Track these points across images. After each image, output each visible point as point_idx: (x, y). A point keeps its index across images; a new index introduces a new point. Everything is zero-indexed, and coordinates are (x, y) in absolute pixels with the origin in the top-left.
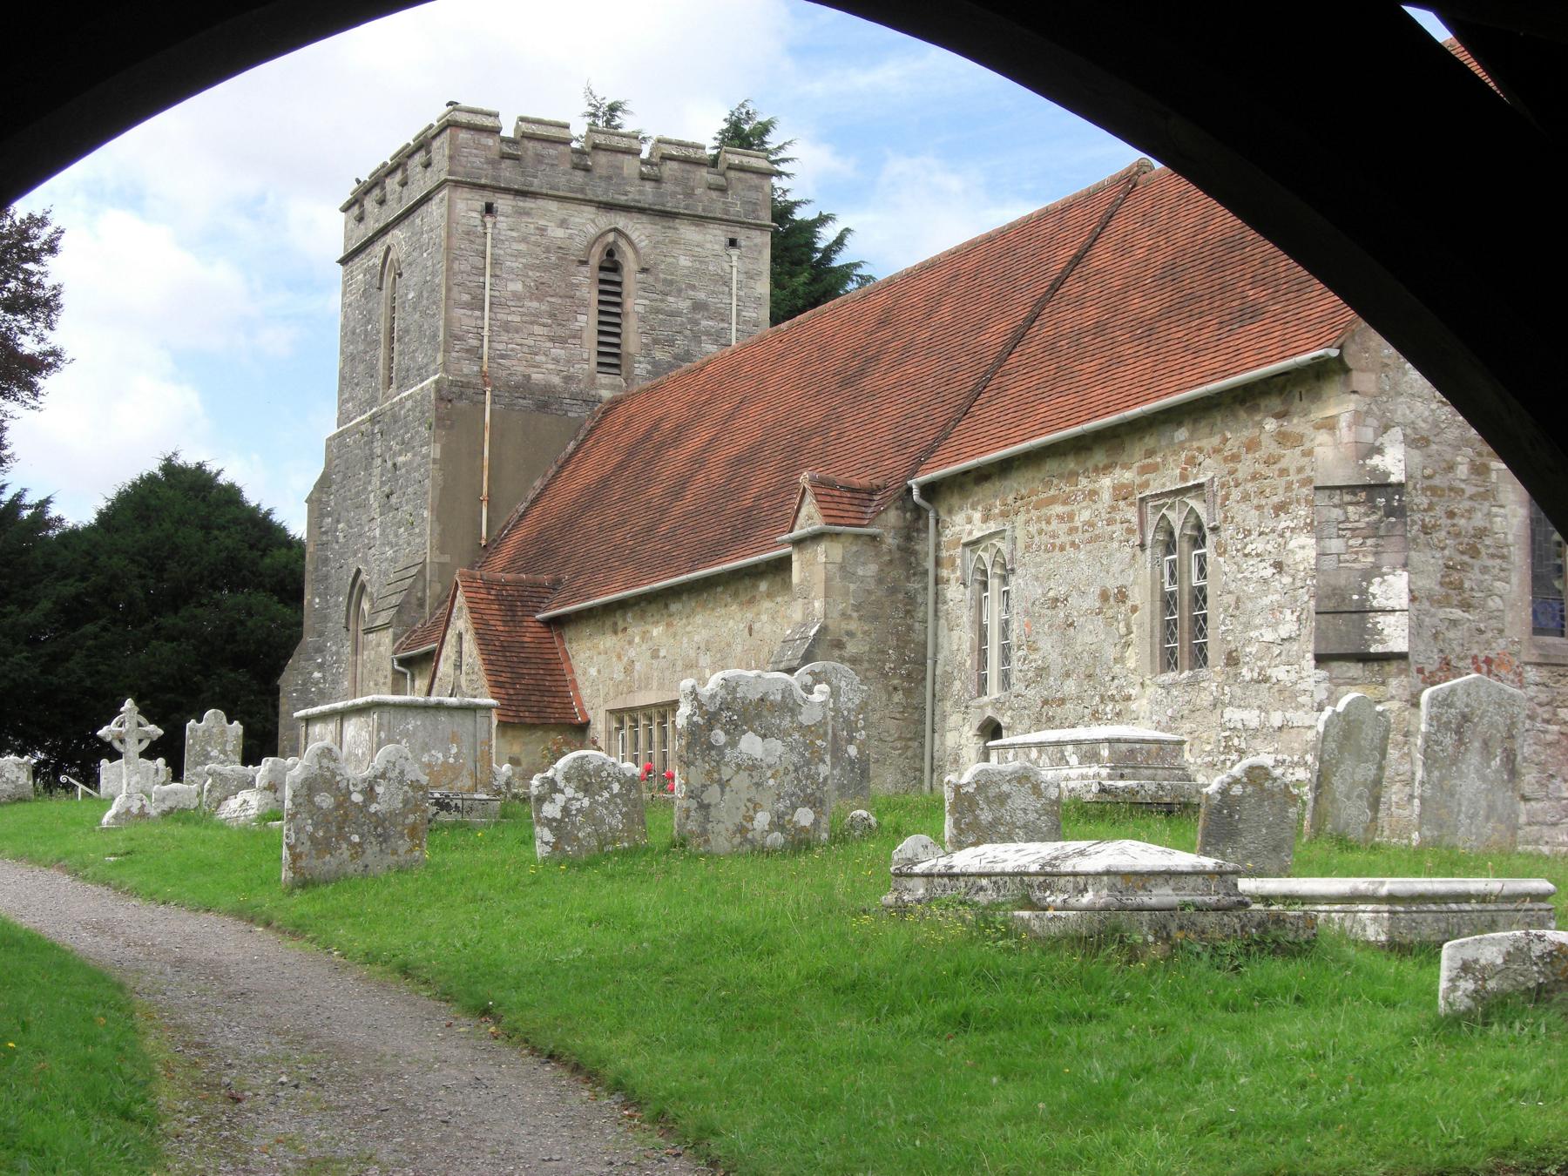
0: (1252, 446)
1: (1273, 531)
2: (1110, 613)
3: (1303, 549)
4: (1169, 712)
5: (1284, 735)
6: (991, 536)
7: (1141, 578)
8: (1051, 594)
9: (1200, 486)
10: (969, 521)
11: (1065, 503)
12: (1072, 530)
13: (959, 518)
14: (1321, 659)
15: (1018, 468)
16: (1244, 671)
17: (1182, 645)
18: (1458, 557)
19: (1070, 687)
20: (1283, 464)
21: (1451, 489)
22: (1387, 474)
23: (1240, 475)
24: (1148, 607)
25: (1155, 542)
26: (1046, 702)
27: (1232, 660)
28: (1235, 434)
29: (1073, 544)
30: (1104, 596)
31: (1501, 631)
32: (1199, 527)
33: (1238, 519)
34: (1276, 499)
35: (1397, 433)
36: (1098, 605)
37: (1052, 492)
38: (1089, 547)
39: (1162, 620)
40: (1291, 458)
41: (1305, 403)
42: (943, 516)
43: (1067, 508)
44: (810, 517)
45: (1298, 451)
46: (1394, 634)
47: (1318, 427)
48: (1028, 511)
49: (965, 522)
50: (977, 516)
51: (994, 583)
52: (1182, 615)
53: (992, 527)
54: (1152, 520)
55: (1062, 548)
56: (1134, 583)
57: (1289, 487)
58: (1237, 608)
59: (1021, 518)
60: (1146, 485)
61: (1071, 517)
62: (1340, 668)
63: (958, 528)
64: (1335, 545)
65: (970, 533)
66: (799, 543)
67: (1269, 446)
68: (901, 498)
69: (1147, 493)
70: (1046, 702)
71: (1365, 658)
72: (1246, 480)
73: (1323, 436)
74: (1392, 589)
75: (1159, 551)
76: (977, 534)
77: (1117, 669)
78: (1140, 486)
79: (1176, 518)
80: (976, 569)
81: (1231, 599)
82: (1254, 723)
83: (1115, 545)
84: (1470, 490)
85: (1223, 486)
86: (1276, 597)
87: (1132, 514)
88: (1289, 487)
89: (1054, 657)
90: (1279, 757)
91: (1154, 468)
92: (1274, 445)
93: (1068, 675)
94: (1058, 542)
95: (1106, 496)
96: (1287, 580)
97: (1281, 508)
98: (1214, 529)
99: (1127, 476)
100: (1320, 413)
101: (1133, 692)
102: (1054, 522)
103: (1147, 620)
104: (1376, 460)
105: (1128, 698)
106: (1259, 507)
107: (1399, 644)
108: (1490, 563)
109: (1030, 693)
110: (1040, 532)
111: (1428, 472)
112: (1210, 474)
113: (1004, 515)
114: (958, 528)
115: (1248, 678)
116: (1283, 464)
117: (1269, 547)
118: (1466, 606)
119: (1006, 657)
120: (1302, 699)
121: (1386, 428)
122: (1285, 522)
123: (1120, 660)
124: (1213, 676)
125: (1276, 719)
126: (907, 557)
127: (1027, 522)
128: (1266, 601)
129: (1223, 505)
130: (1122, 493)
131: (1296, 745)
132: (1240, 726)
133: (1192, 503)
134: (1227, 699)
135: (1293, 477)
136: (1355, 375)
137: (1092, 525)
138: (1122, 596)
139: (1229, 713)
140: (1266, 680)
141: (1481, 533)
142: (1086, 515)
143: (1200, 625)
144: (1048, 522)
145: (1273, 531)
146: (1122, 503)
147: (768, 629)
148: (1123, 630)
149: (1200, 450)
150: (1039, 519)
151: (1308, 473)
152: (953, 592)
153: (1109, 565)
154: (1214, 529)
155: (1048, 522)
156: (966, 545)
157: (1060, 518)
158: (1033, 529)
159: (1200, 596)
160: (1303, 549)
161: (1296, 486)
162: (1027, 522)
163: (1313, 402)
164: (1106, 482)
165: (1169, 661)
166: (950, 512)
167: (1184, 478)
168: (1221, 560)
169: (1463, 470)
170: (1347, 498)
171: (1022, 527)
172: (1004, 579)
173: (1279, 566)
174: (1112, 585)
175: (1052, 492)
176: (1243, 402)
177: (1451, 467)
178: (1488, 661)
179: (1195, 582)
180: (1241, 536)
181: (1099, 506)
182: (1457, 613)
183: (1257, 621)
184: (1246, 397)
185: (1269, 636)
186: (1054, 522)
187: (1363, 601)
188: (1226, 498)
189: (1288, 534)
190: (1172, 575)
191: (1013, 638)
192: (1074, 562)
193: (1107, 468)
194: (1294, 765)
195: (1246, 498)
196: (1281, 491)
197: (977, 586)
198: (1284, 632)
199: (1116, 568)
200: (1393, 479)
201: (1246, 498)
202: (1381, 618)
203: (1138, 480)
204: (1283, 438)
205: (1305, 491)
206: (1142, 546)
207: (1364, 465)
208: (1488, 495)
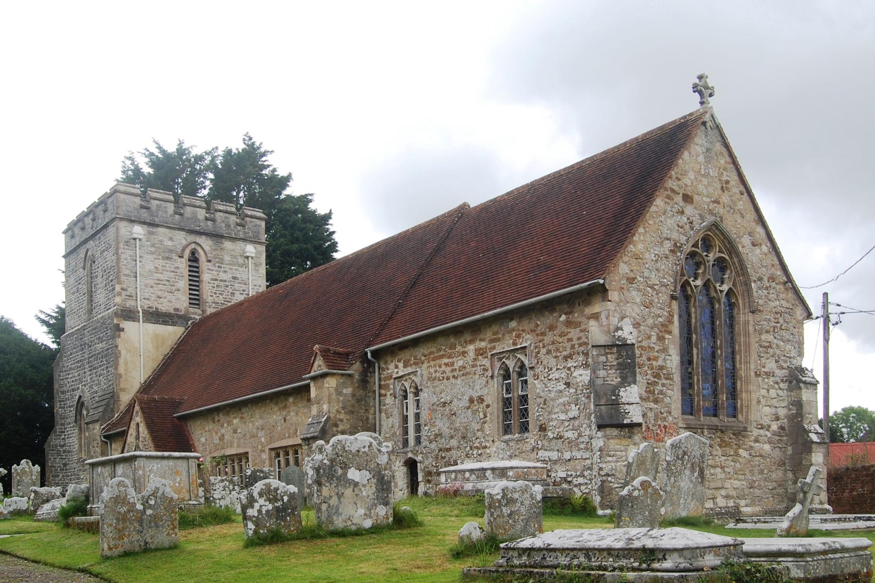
0: (552, 328)
1: (564, 368)
2: (475, 408)
3: (583, 376)
4: (508, 453)
5: (571, 462)
6: (409, 374)
7: (492, 392)
8: (442, 400)
9: (525, 348)
10: (397, 367)
11: (449, 357)
12: (452, 371)
13: (391, 366)
14: (600, 427)
15: (423, 342)
16: (549, 434)
17: (515, 422)
18: (652, 379)
19: (454, 443)
20: (569, 336)
21: (649, 347)
22: (625, 339)
23: (545, 342)
24: (495, 405)
25: (499, 374)
26: (440, 450)
27: (543, 429)
28: (543, 322)
29: (454, 377)
30: (471, 400)
31: (670, 413)
32: (522, 366)
33: (545, 362)
34: (565, 353)
35: (627, 320)
36: (468, 405)
37: (442, 353)
38: (463, 378)
39: (518, 409)
40: (574, 333)
41: (581, 307)
42: (382, 365)
43: (451, 360)
44: (319, 366)
45: (578, 330)
46: (635, 415)
47: (589, 318)
48: (429, 362)
49: (395, 368)
50: (401, 365)
51: (410, 396)
52: (514, 409)
53: (409, 370)
54: (498, 365)
55: (448, 379)
56: (488, 394)
57: (573, 347)
58: (545, 404)
59: (425, 365)
60: (494, 348)
61: (452, 364)
62: (609, 431)
63: (390, 371)
64: (602, 373)
65: (397, 373)
67: (561, 328)
68: (361, 357)
69: (495, 352)
70: (440, 450)
71: (621, 426)
72: (549, 344)
73: (592, 323)
74: (631, 394)
75: (501, 379)
76: (401, 374)
77: (479, 434)
78: (490, 349)
79: (511, 364)
80: (400, 389)
81: (543, 400)
82: (555, 458)
83: (477, 376)
84: (657, 348)
85: (536, 347)
86: (567, 399)
87: (486, 362)
88: (573, 347)
89: (446, 431)
90: (569, 473)
91: (498, 340)
92: (564, 327)
93: (452, 437)
94: (445, 375)
95: (472, 354)
96: (572, 390)
97: (566, 358)
98: (532, 368)
99: (483, 344)
100: (589, 311)
101: (488, 445)
102: (443, 367)
103: (495, 411)
104: (620, 333)
105: (486, 447)
106: (556, 357)
107: (637, 419)
108: (665, 382)
110: (436, 372)
111: (640, 339)
112: (529, 342)
113: (415, 364)
114: (390, 371)
115: (551, 437)
116: (569, 336)
117: (562, 376)
118: (656, 401)
119: (418, 428)
120: (582, 446)
121: (622, 318)
122: (570, 363)
123: (481, 430)
124: (532, 438)
125: (567, 455)
126: (364, 382)
127: (428, 367)
128: (561, 401)
129: (536, 356)
130: (480, 352)
131: (578, 468)
132: (547, 459)
133: (519, 356)
134: (540, 447)
135: (575, 342)
136: (610, 293)
137: (465, 367)
138: (481, 400)
139: (541, 453)
140: (561, 437)
141: (661, 368)
142: (460, 363)
143: (524, 413)
144: (440, 367)
145: (564, 368)
146: (480, 357)
148: (482, 416)
149: (523, 331)
150: (435, 366)
151: (584, 340)
152: (389, 400)
153: (474, 386)
154: (532, 368)
155: (440, 367)
156: (395, 379)
157: (446, 365)
158: (432, 370)
159: (524, 399)
160: (583, 376)
161: (577, 346)
162: (428, 367)
163: (586, 306)
165: (507, 430)
166: (386, 363)
167: (515, 344)
168: (536, 382)
169: (654, 339)
170: (608, 351)
171: (424, 370)
172: (416, 394)
173: (568, 384)
174: (475, 395)
175: (442, 353)
176: (546, 308)
177: (649, 337)
178: (665, 427)
179: (520, 393)
180: (547, 370)
181: (468, 358)
182: (652, 405)
183: (556, 410)
184: (549, 306)
185: (563, 417)
186: (443, 367)
187: (617, 400)
188: (538, 352)
189: (573, 369)
190: (507, 390)
191: (422, 421)
192: (456, 384)
193: (472, 342)
194: (577, 476)
195: (549, 352)
196: (568, 349)
197: (401, 397)
198: (571, 414)
199: (478, 387)
200: (629, 342)
201: (549, 352)
202: (627, 406)
203: (489, 346)
204: (568, 323)
205: (582, 348)
206: (492, 377)
207: (614, 336)
208: (664, 350)
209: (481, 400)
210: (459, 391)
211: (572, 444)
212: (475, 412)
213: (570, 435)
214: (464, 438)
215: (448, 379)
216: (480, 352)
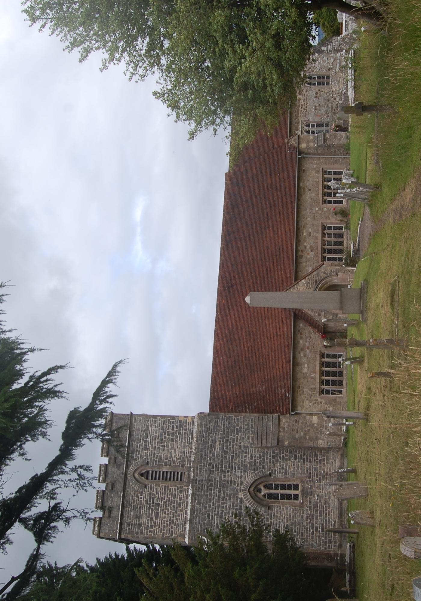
7: (316, 88)
17: (325, 81)
19: (330, 105)
27: (329, 69)
30: (316, 97)
52: (321, 80)
61: (302, 105)
66: (298, 144)
109: (330, 115)
125: (338, 61)
130: (300, 93)
139: (337, 70)
142: (302, 101)
147: (310, 182)
157: (302, 108)
159: (319, 78)
164: (299, 97)
165: (328, 84)
171: (301, 119)
185: (327, 62)
198: (326, 60)
199: (312, 94)
209: (317, 93)
210: (312, 102)
211: (335, 59)
212: (320, 96)
213: (332, 60)
214: (329, 101)
215: (307, 107)
216: (300, 93)
